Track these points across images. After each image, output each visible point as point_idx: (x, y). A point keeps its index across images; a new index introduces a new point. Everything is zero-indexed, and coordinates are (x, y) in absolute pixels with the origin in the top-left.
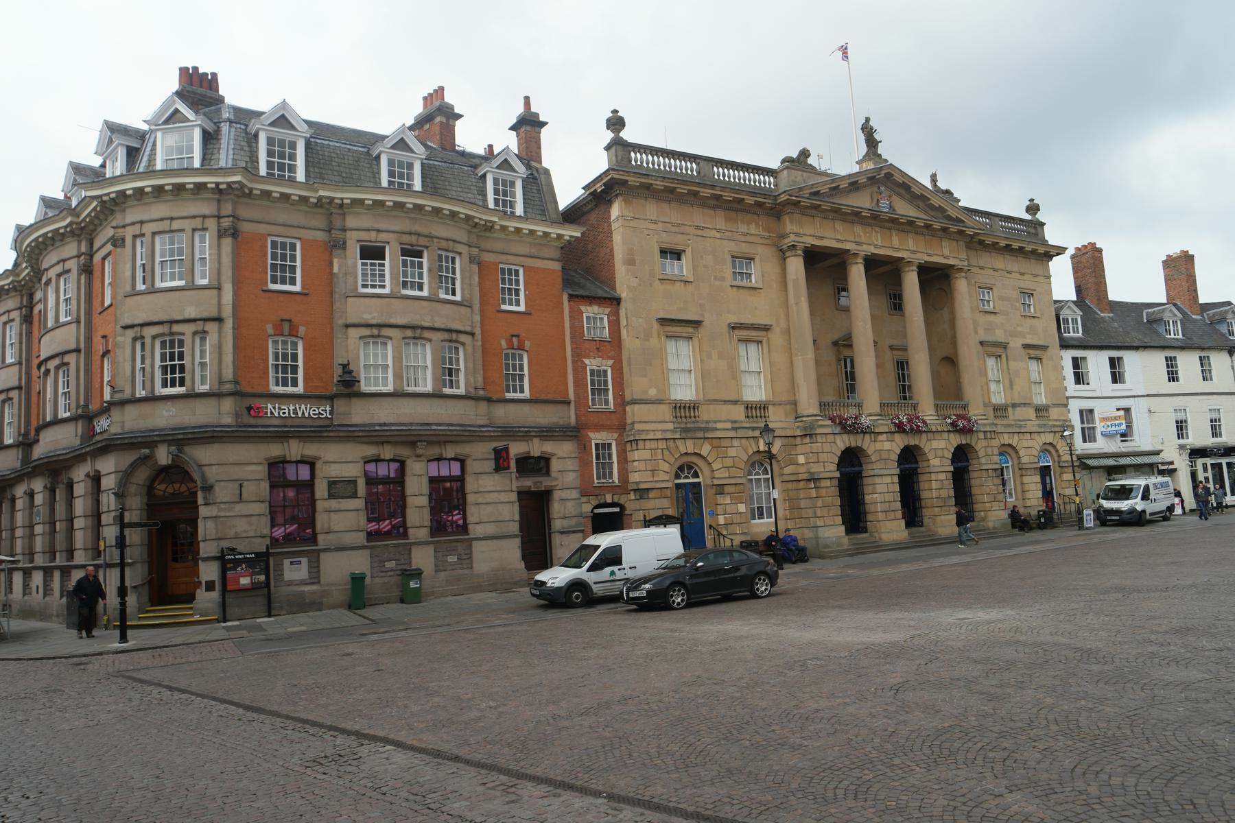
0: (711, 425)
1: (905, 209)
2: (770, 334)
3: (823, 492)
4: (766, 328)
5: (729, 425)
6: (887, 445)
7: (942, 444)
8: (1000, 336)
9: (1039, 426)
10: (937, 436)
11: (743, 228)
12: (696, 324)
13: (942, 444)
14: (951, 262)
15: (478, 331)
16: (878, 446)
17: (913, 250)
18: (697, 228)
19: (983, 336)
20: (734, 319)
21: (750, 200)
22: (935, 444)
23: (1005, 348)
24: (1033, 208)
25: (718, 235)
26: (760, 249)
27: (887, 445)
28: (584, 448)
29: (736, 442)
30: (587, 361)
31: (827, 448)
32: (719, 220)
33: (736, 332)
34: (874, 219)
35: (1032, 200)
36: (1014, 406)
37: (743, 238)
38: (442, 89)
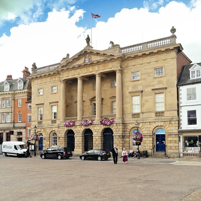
0: (44, 125)
1: (95, 59)
2: (58, 103)
3: (60, 140)
4: (58, 102)
5: (47, 125)
6: (79, 129)
7: (98, 128)
8: (140, 88)
9: (155, 120)
10: (96, 126)
11: (54, 80)
12: (43, 104)
13: (98, 128)
14: (112, 69)
15: (13, 112)
16: (77, 129)
17: (96, 71)
18: (45, 83)
19: (130, 89)
20: (51, 101)
21: (52, 73)
22: (95, 128)
23: (142, 91)
24: (173, 30)
25: (49, 83)
26: (58, 83)
27: (79, 129)
28: (27, 130)
29: (48, 129)
30: (28, 114)
31: (62, 130)
32: (48, 79)
33: (51, 104)
34: (80, 67)
35: (173, 27)
36: (143, 113)
37: (54, 82)
38: (25, 67)
